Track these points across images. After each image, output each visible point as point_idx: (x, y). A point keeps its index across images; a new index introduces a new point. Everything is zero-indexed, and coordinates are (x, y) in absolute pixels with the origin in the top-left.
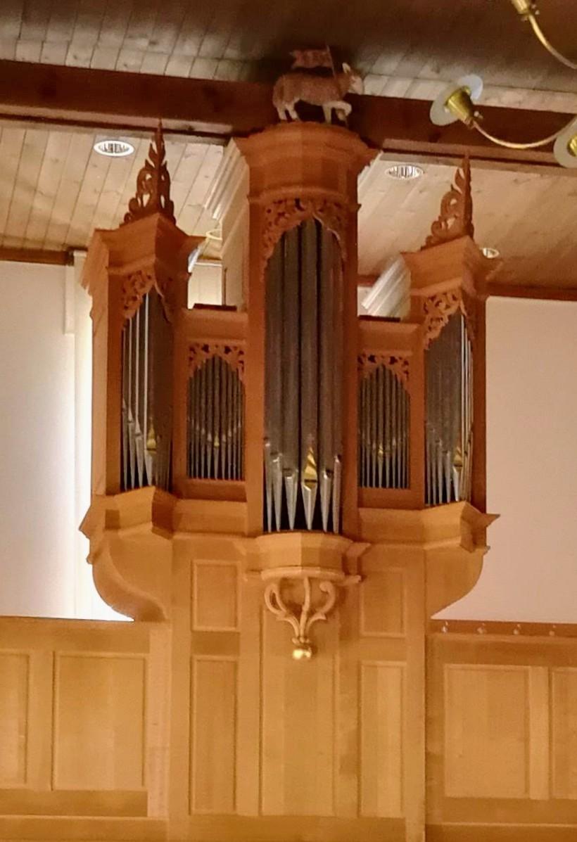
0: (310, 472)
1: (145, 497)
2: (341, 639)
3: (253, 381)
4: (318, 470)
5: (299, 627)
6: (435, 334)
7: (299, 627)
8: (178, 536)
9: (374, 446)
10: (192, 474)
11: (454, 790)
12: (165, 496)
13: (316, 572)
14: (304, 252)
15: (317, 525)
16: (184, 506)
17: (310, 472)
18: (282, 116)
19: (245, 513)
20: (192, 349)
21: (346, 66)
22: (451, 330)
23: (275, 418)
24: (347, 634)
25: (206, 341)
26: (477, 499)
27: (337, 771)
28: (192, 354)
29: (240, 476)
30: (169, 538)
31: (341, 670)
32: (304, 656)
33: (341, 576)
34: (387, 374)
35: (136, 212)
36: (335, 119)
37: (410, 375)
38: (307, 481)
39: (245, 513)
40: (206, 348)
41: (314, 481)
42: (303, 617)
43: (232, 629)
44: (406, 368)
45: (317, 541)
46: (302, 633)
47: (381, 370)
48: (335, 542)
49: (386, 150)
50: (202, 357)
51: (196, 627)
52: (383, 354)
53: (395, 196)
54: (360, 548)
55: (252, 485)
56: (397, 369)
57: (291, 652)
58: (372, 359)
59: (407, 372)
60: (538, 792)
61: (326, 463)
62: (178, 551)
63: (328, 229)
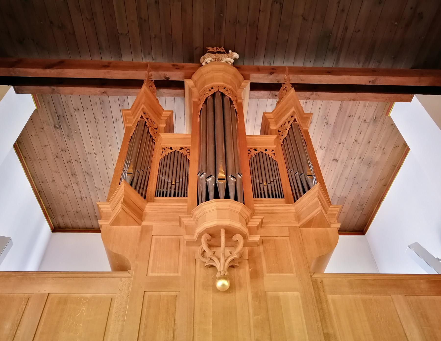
4: (227, 175)
5: (221, 266)
6: (285, 135)
8: (144, 223)
10: (158, 194)
13: (227, 222)
16: (148, 207)
17: (222, 175)
18: (204, 64)
20: (164, 149)
24: (255, 275)
25: (171, 145)
28: (163, 150)
29: (185, 194)
30: (140, 224)
31: (253, 298)
32: (223, 285)
33: (246, 231)
34: (264, 155)
38: (219, 179)
40: (171, 148)
41: (224, 179)
42: (222, 260)
43: (176, 274)
44: (273, 152)
46: (222, 269)
47: (260, 153)
48: (238, 206)
51: (150, 274)
57: (214, 286)
58: (256, 150)
59: (274, 154)
61: (230, 172)
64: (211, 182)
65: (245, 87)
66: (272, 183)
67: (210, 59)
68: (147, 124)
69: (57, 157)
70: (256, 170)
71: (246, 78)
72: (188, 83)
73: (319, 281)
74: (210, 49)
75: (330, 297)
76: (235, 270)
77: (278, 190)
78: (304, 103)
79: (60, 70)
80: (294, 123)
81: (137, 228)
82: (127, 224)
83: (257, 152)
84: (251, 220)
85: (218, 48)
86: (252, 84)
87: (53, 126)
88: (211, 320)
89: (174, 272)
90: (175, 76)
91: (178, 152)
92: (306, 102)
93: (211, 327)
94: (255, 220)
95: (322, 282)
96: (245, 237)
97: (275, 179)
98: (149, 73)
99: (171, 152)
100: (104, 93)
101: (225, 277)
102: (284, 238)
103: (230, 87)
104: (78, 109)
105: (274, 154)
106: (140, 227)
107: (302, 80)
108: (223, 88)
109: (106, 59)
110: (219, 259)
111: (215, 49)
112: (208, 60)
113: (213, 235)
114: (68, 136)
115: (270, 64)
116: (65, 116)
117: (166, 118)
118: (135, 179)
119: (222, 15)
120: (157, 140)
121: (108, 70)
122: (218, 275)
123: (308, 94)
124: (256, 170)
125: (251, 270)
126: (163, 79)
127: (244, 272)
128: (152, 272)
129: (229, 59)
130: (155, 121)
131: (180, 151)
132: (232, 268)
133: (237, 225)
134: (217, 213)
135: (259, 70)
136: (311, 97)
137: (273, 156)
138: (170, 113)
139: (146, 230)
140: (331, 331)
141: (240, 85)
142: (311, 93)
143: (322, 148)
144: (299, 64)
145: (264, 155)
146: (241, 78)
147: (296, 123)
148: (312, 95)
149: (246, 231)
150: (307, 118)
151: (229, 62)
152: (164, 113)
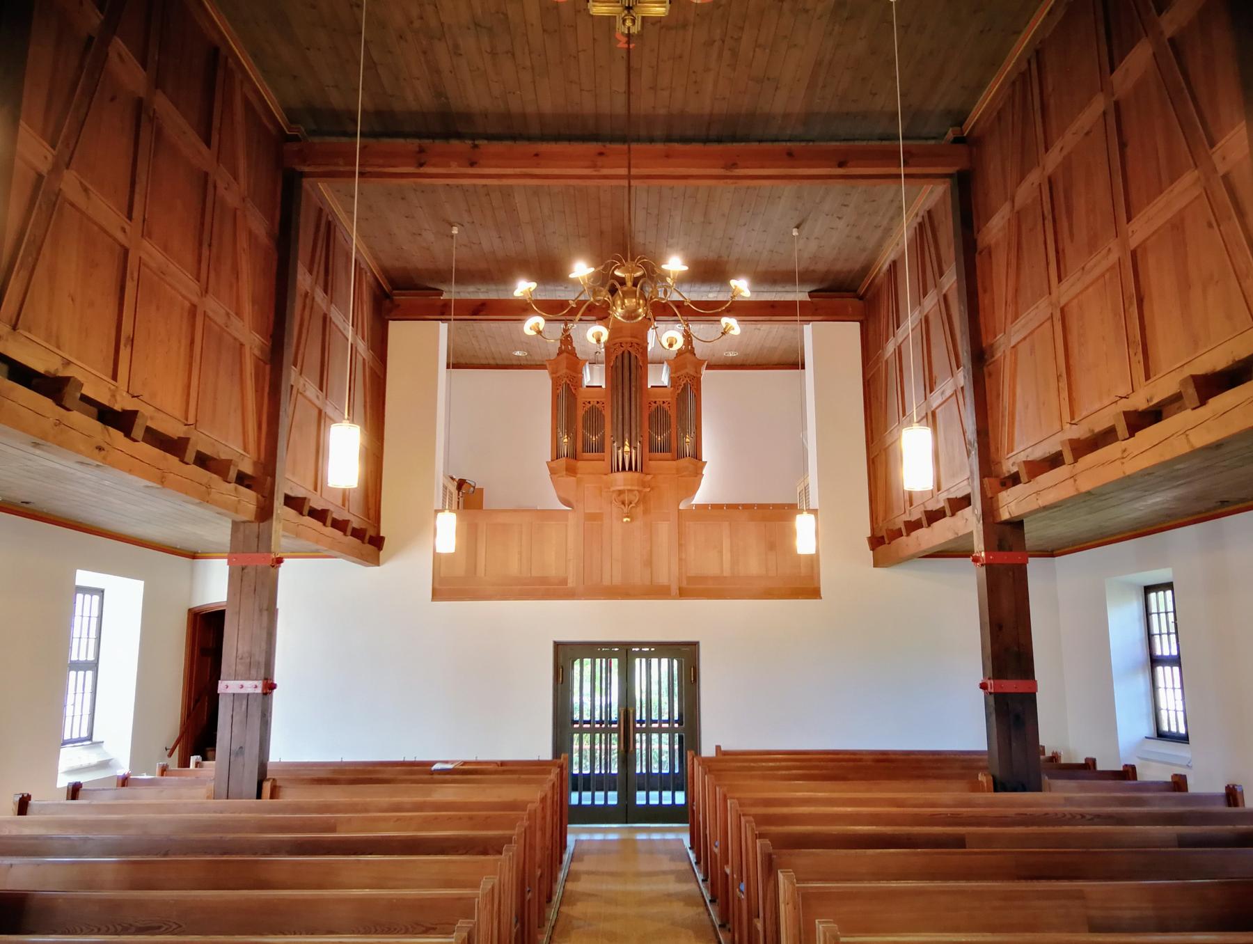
0: (627, 448)
1: (563, 461)
3: (607, 414)
5: (626, 510)
7: (626, 510)
11: (692, 573)
12: (572, 462)
14: (627, 361)
15: (630, 469)
16: (580, 464)
17: (627, 448)
19: (603, 466)
22: (684, 389)
23: (615, 428)
24: (646, 512)
26: (697, 455)
35: (560, 352)
39: (603, 466)
45: (628, 475)
48: (637, 475)
52: (659, 400)
53: (666, 337)
54: (649, 477)
55: (607, 455)
56: (666, 406)
60: (727, 573)
62: (579, 482)
63: (633, 353)
103: (635, 340)
113: (621, 492)
127: (640, 509)
134: (621, 480)
139: (579, 482)
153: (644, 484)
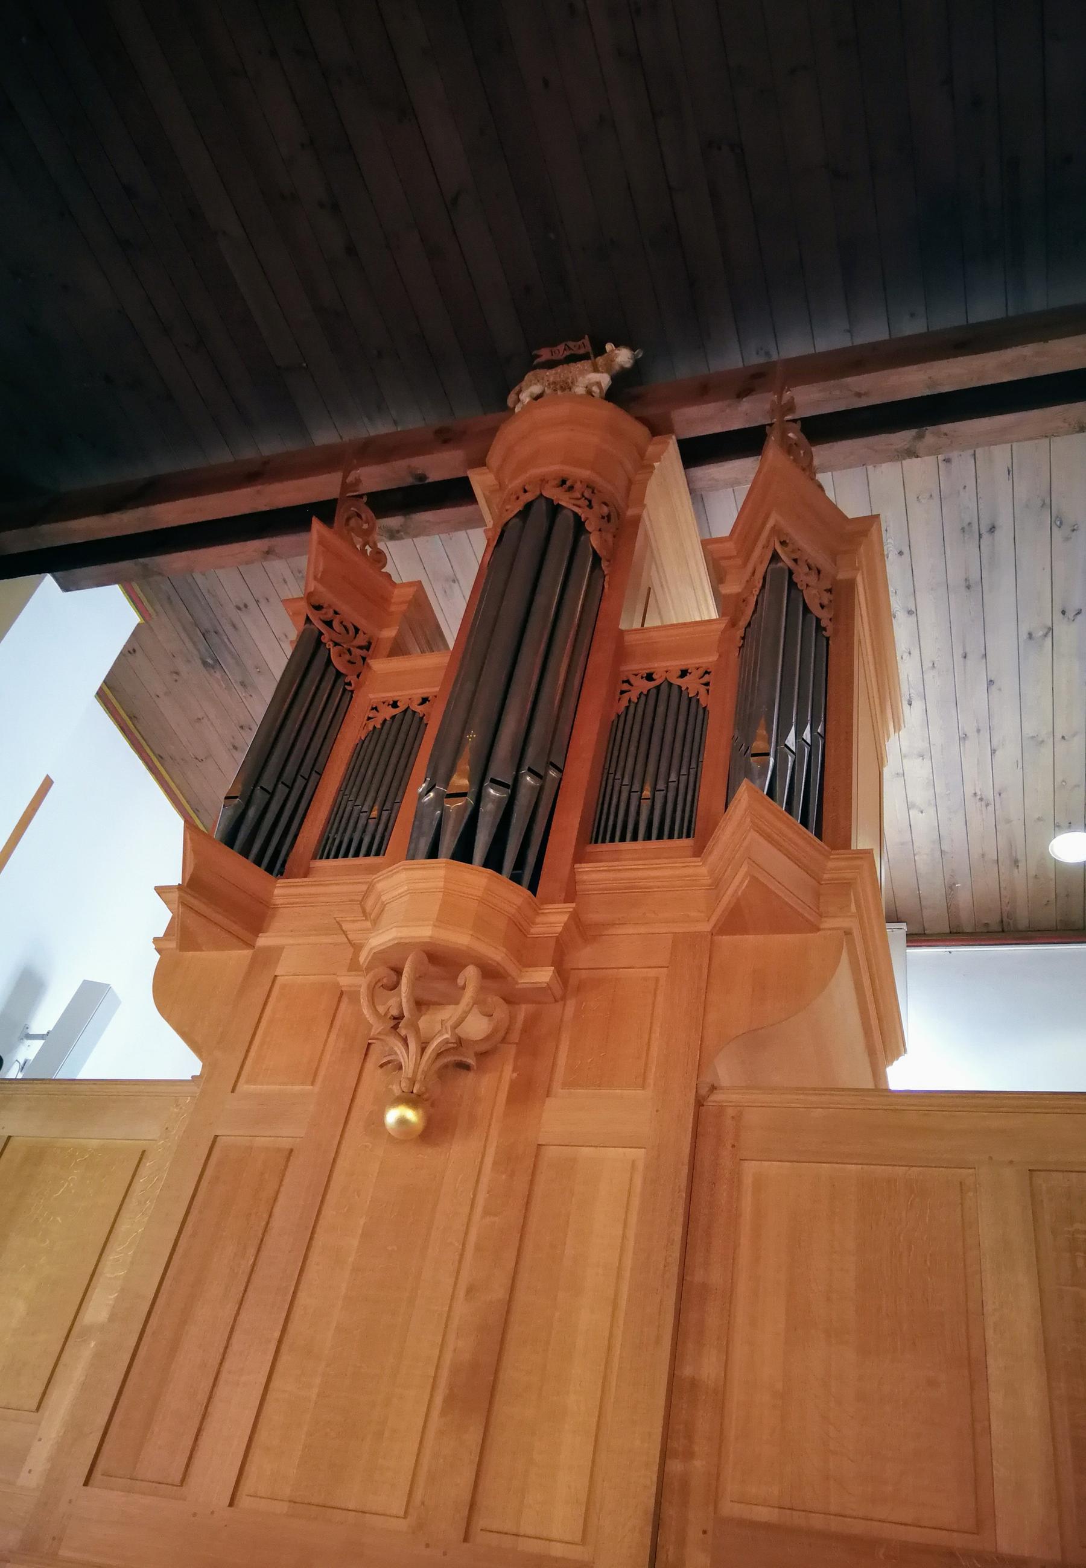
2: (511, 1099)
9: (636, 787)
17: (460, 782)
21: (609, 347)
24: (526, 1093)
27: (439, 1400)
30: (251, 946)
32: (402, 1122)
36: (590, 393)
37: (711, 688)
44: (706, 678)
47: (664, 688)
48: (475, 878)
49: (697, 452)
50: (388, 712)
52: (665, 667)
54: (555, 918)
56: (691, 684)
58: (650, 677)
64: (495, 800)
65: (658, 459)
66: (672, 786)
67: (536, 389)
68: (325, 639)
69: (235, 748)
70: (633, 749)
71: (657, 429)
72: (480, 481)
73: (730, 1112)
74: (545, 354)
75: (750, 1169)
76: (471, 1075)
77: (683, 811)
78: (942, 465)
79: (140, 512)
80: (773, 566)
81: (240, 956)
82: (219, 946)
83: (652, 684)
84: (539, 919)
85: (571, 344)
86: (683, 444)
87: (199, 662)
88: (362, 1221)
89: (303, 1084)
90: (439, 466)
91: (414, 712)
92: (947, 461)
93: (355, 1243)
94: (552, 918)
95: (737, 1118)
96: (490, 973)
97: (684, 771)
98: (345, 477)
99: (393, 717)
100: (268, 553)
101: (411, 1100)
102: (652, 973)
103: (586, 473)
104: (246, 606)
105: (707, 684)
106: (247, 953)
107: (859, 395)
108: (558, 482)
109: (271, 447)
110: (405, 1040)
111: (561, 351)
112: (525, 397)
114: (243, 684)
115: (767, 354)
116: (219, 628)
117: (404, 607)
118: (252, 813)
119: (552, 236)
120: (359, 686)
121: (259, 487)
122: (396, 1090)
123: (902, 438)
124: (633, 749)
125: (515, 1075)
126: (410, 481)
128: (248, 1082)
129: (594, 377)
130: (362, 623)
131: (419, 709)
132: (464, 1072)
133: (460, 938)
135: (703, 391)
136: (921, 446)
137: (702, 690)
138: (412, 590)
140: (716, 1277)
141: (642, 454)
142: (913, 432)
143: (1071, 614)
144: (873, 332)
145: (675, 692)
146: (640, 431)
147: (780, 564)
148: (920, 437)
149: (496, 954)
150: (856, 536)
151: (595, 389)
152: (396, 592)
153: (522, 945)
